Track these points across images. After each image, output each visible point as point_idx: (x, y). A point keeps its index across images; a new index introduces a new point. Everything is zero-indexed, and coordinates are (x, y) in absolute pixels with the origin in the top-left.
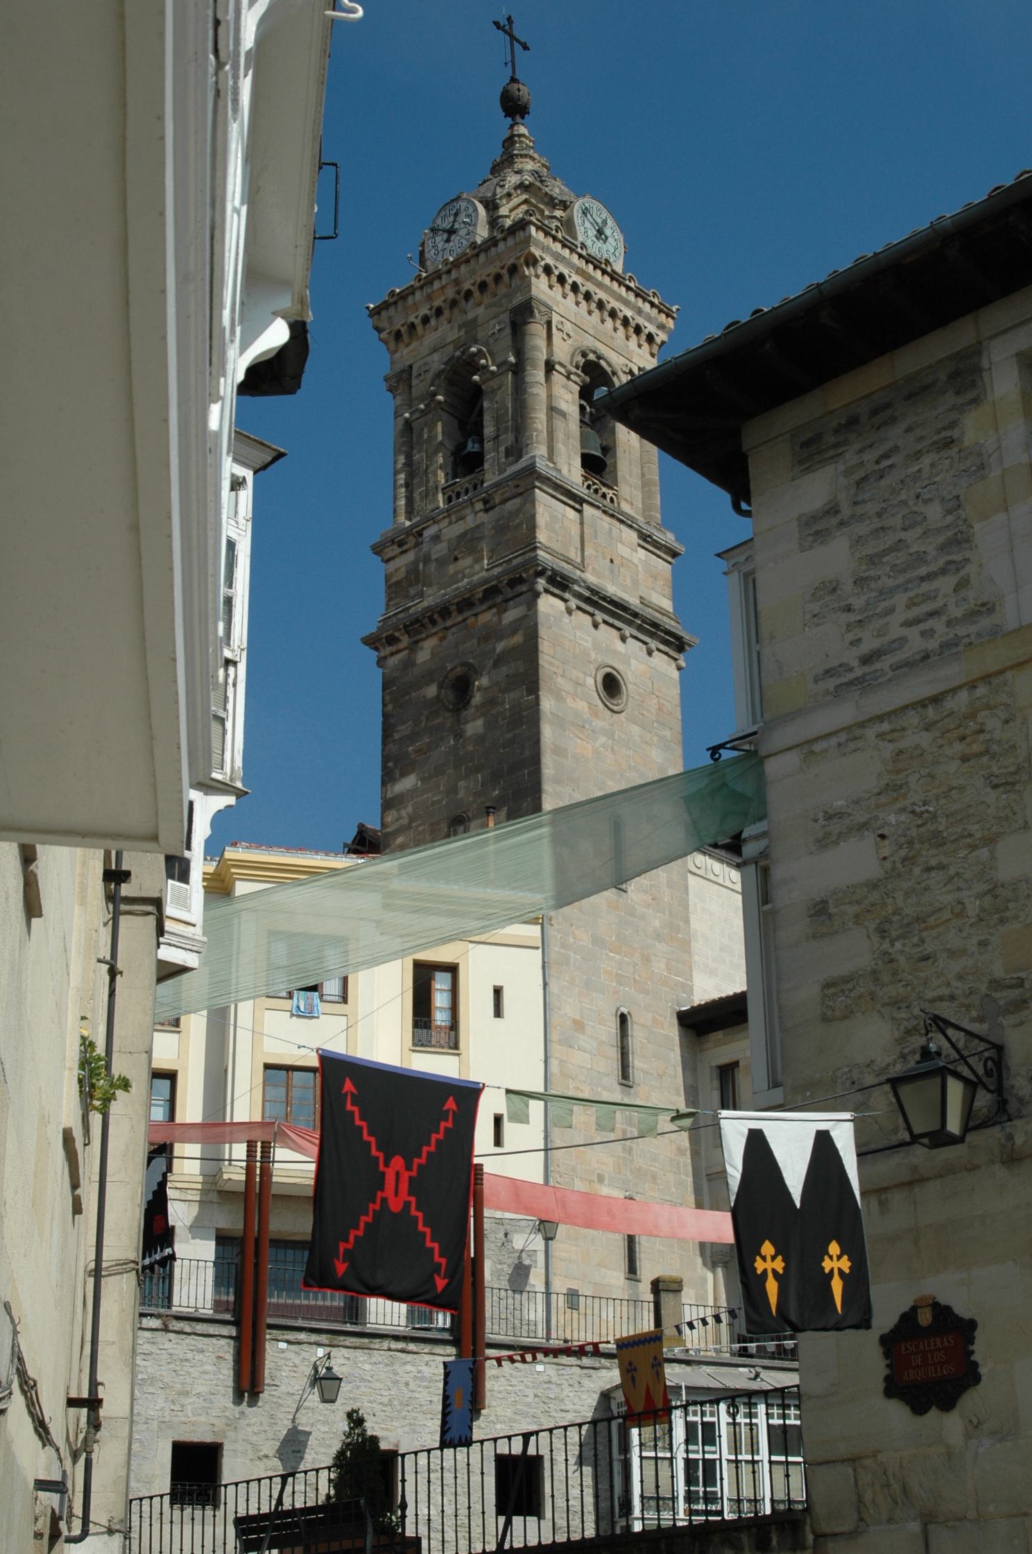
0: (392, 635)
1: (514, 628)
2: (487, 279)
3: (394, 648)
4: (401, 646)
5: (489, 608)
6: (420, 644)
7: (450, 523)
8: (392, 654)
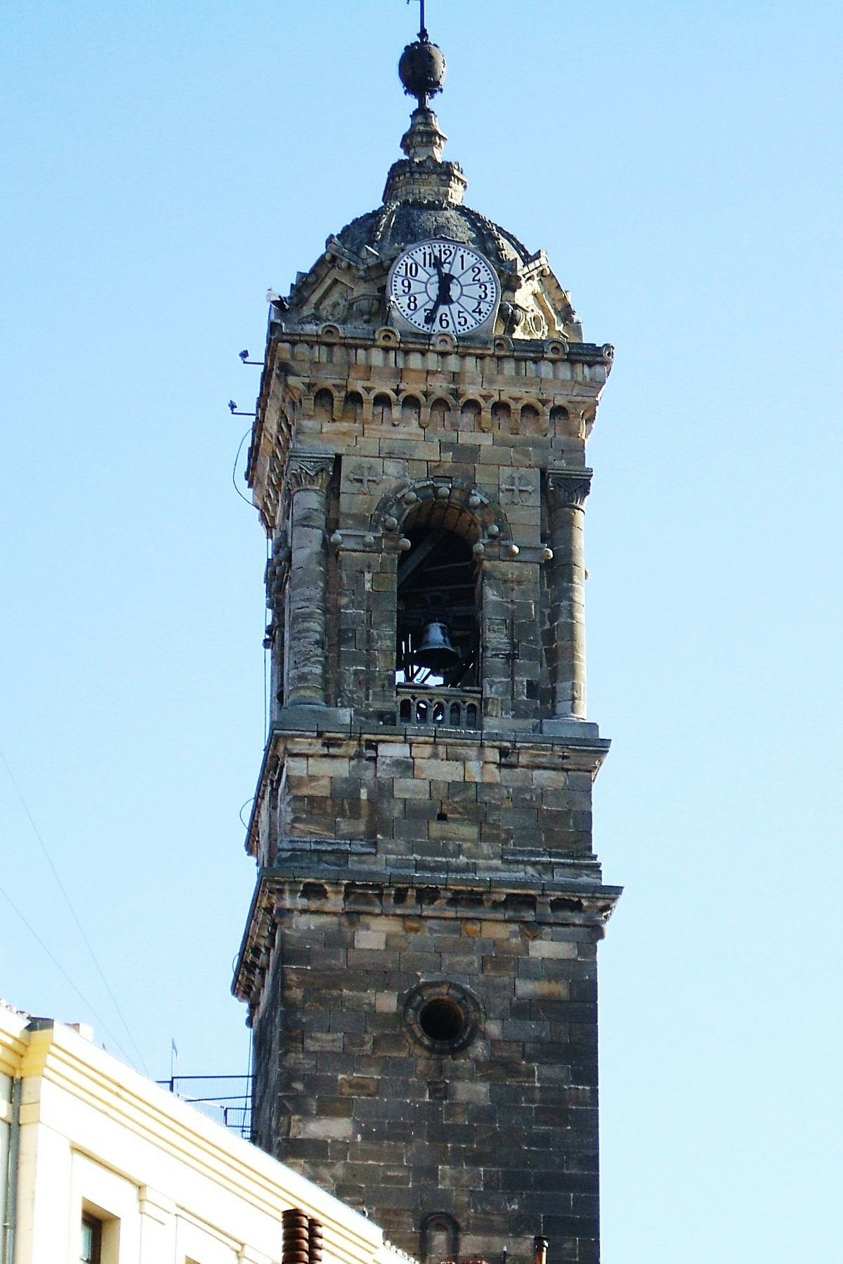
0: (322, 886)
1: (553, 969)
2: (513, 405)
3: (314, 904)
4: (329, 907)
5: (506, 921)
6: (364, 919)
7: (435, 756)
8: (304, 911)
